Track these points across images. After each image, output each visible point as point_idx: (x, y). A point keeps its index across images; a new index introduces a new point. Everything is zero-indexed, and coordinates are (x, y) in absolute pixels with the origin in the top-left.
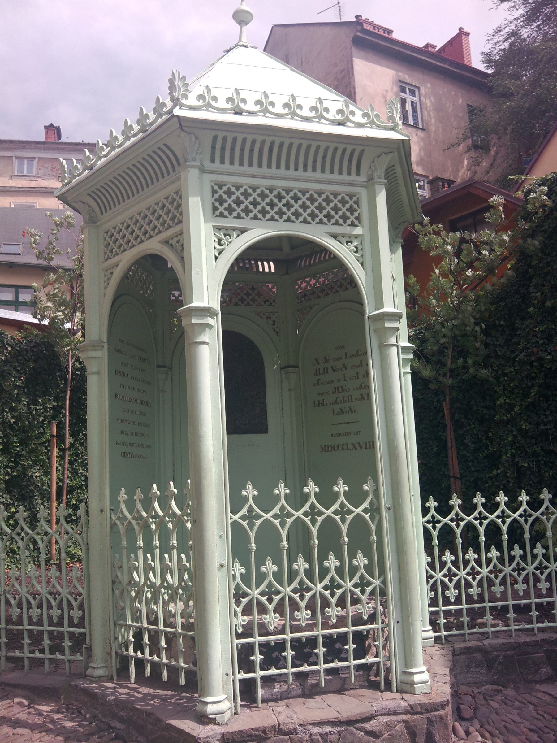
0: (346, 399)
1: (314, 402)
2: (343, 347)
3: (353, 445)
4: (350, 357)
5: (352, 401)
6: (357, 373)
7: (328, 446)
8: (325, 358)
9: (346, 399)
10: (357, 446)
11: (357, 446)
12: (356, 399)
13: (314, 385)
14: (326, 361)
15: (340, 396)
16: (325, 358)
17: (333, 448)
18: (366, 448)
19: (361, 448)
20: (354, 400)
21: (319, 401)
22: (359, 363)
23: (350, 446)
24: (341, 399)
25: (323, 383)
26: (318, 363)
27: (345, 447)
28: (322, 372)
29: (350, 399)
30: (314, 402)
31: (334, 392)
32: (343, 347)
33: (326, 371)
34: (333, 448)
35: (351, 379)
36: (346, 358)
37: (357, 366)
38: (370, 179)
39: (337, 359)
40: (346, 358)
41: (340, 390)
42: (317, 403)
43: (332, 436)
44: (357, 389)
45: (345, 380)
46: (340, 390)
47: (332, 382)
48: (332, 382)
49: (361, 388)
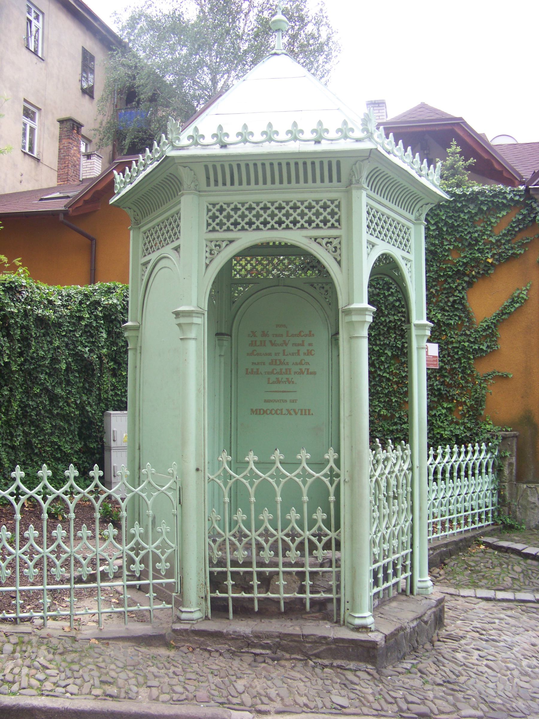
0: (284, 371)
1: (247, 369)
2: (284, 326)
3: (288, 410)
4: (293, 335)
5: (290, 374)
6: (299, 351)
7: (260, 410)
8: (263, 332)
9: (284, 371)
10: (292, 412)
11: (292, 412)
12: (295, 373)
13: (248, 354)
14: (264, 334)
15: (278, 368)
16: (263, 332)
17: (265, 412)
18: (301, 414)
19: (296, 414)
20: (292, 373)
21: (252, 369)
22: (301, 342)
23: (284, 412)
24: (279, 371)
25: (258, 354)
26: (255, 336)
27: (279, 412)
28: (258, 343)
29: (288, 371)
30: (247, 369)
31: (271, 364)
32: (284, 326)
33: (263, 344)
34: (265, 412)
35: (293, 354)
36: (287, 336)
37: (299, 345)
38: (418, 219)
39: (277, 336)
40: (287, 336)
41: (278, 362)
42: (249, 370)
43: (266, 401)
44: (297, 364)
45: (284, 355)
46: (278, 362)
47: (270, 354)
48: (270, 354)
49: (301, 363)
